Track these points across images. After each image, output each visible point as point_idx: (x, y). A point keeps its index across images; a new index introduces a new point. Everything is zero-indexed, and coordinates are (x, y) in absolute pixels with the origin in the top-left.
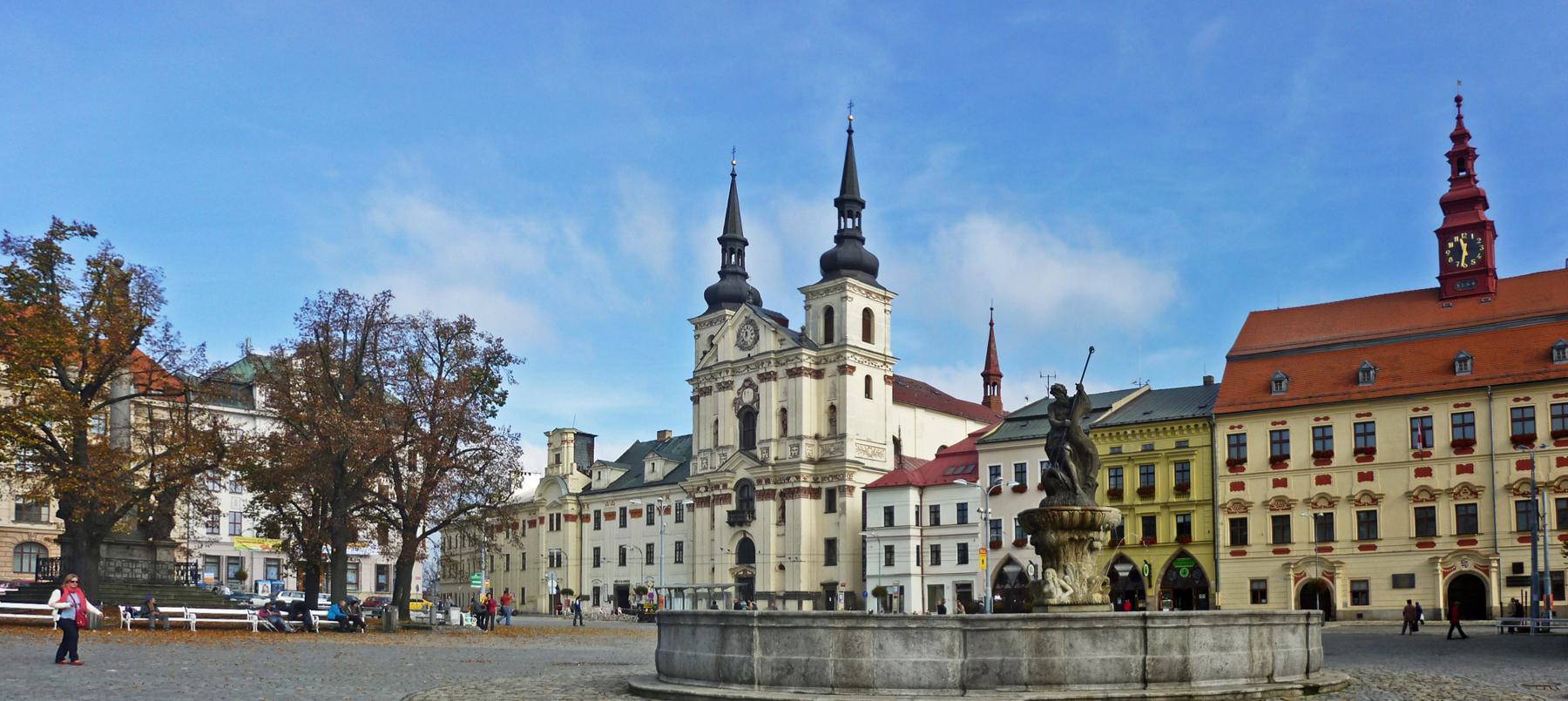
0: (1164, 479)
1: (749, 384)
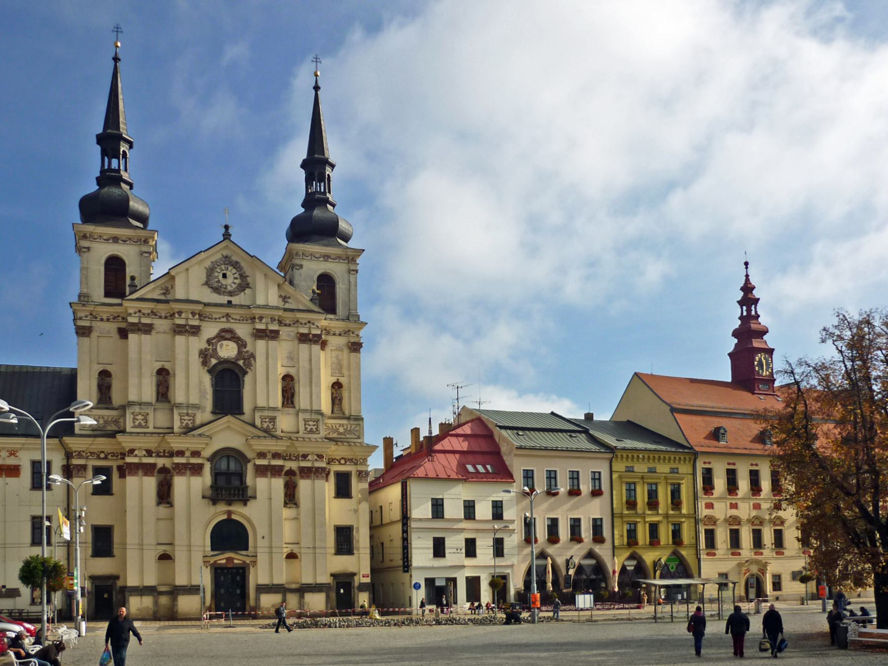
0: (664, 496)
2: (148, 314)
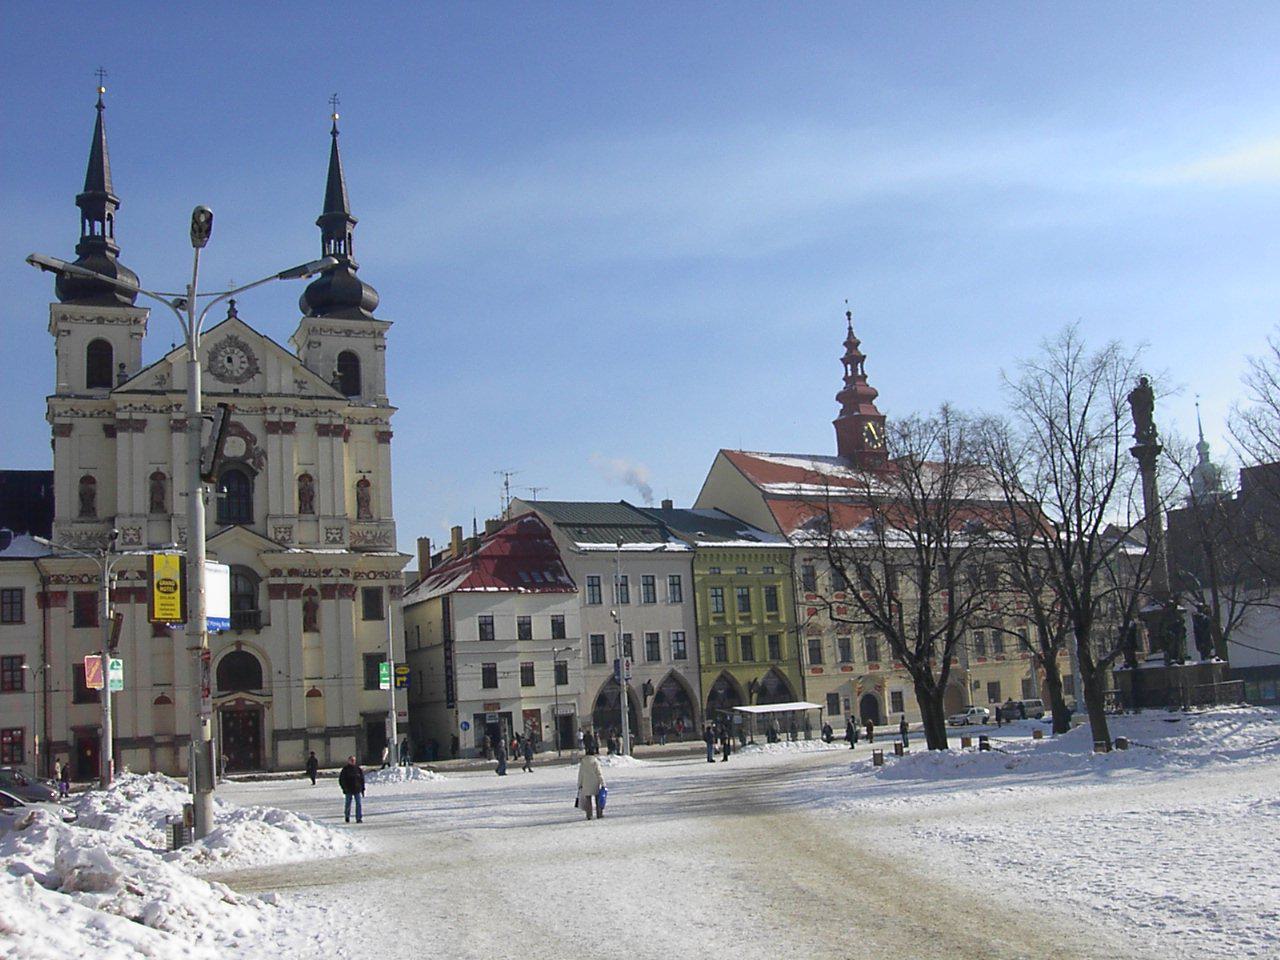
2: (141, 409)
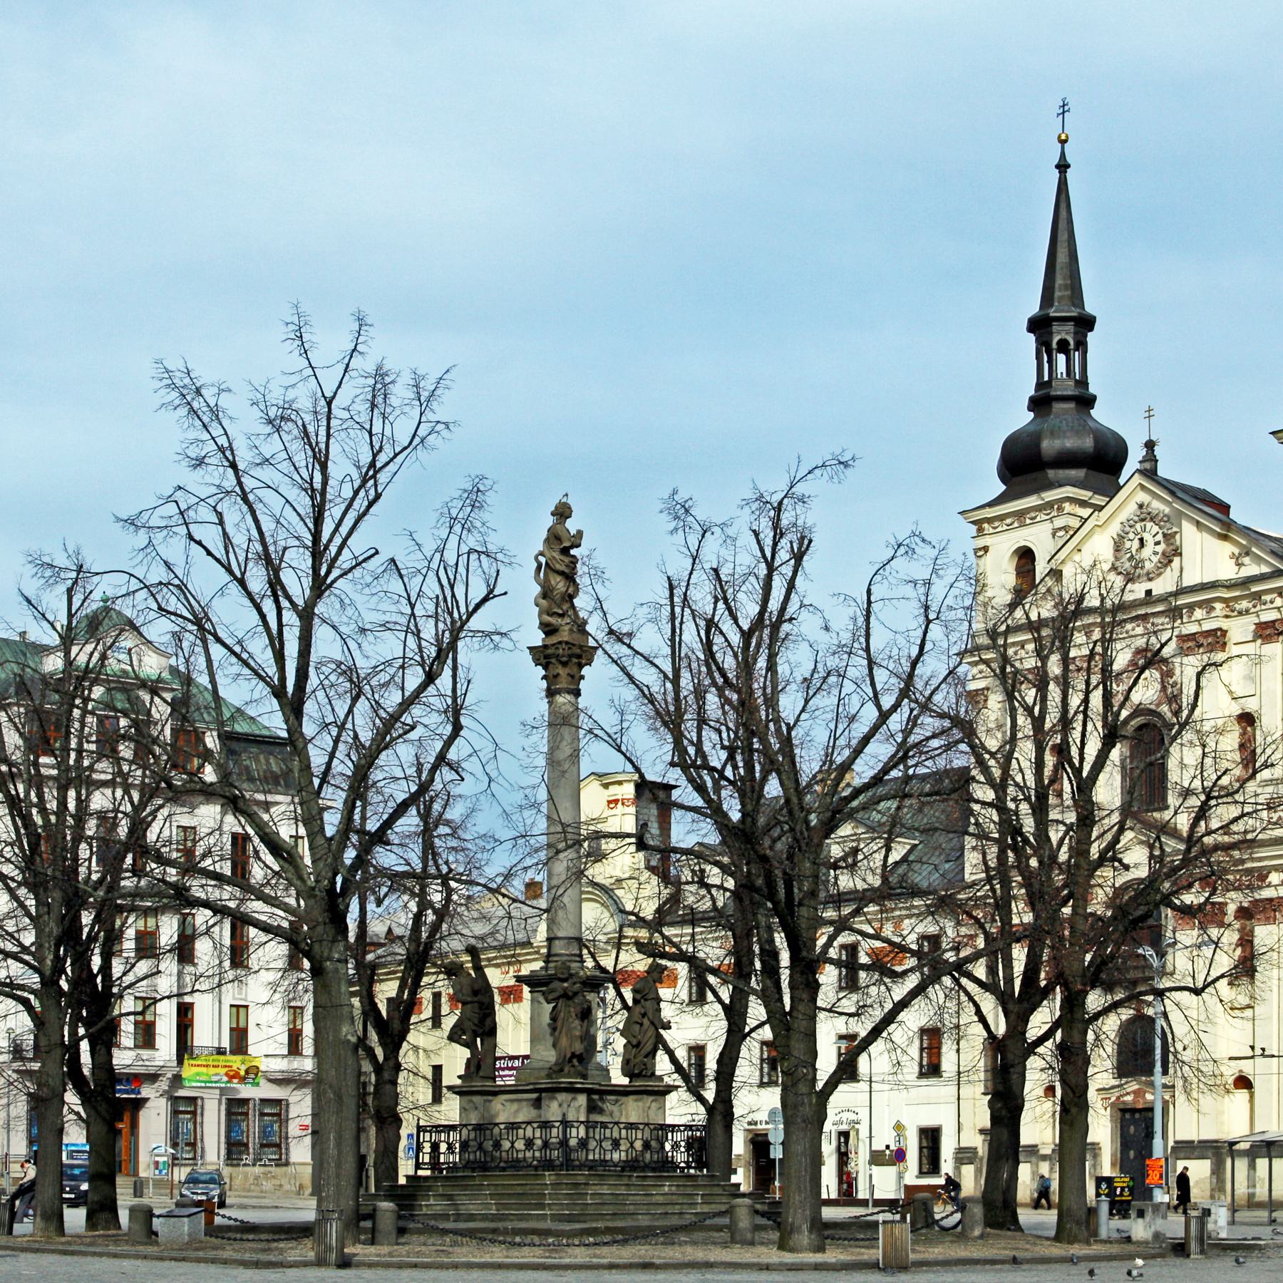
1: (1150, 659)
